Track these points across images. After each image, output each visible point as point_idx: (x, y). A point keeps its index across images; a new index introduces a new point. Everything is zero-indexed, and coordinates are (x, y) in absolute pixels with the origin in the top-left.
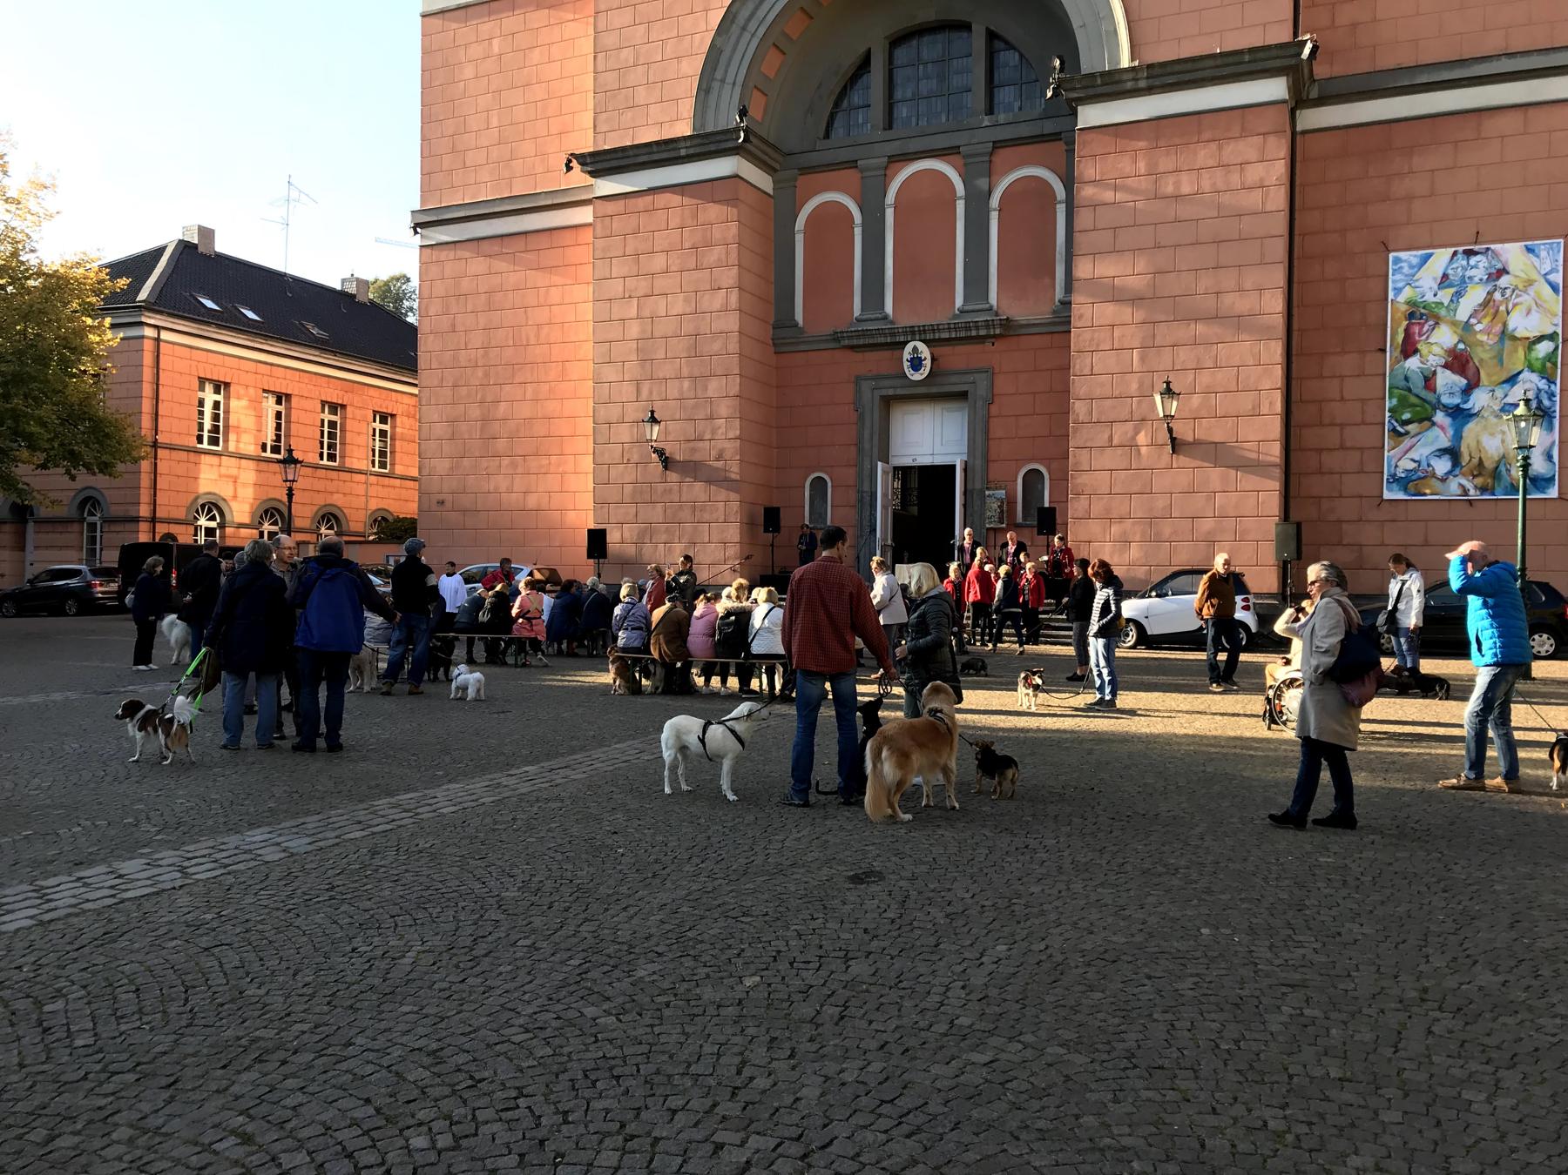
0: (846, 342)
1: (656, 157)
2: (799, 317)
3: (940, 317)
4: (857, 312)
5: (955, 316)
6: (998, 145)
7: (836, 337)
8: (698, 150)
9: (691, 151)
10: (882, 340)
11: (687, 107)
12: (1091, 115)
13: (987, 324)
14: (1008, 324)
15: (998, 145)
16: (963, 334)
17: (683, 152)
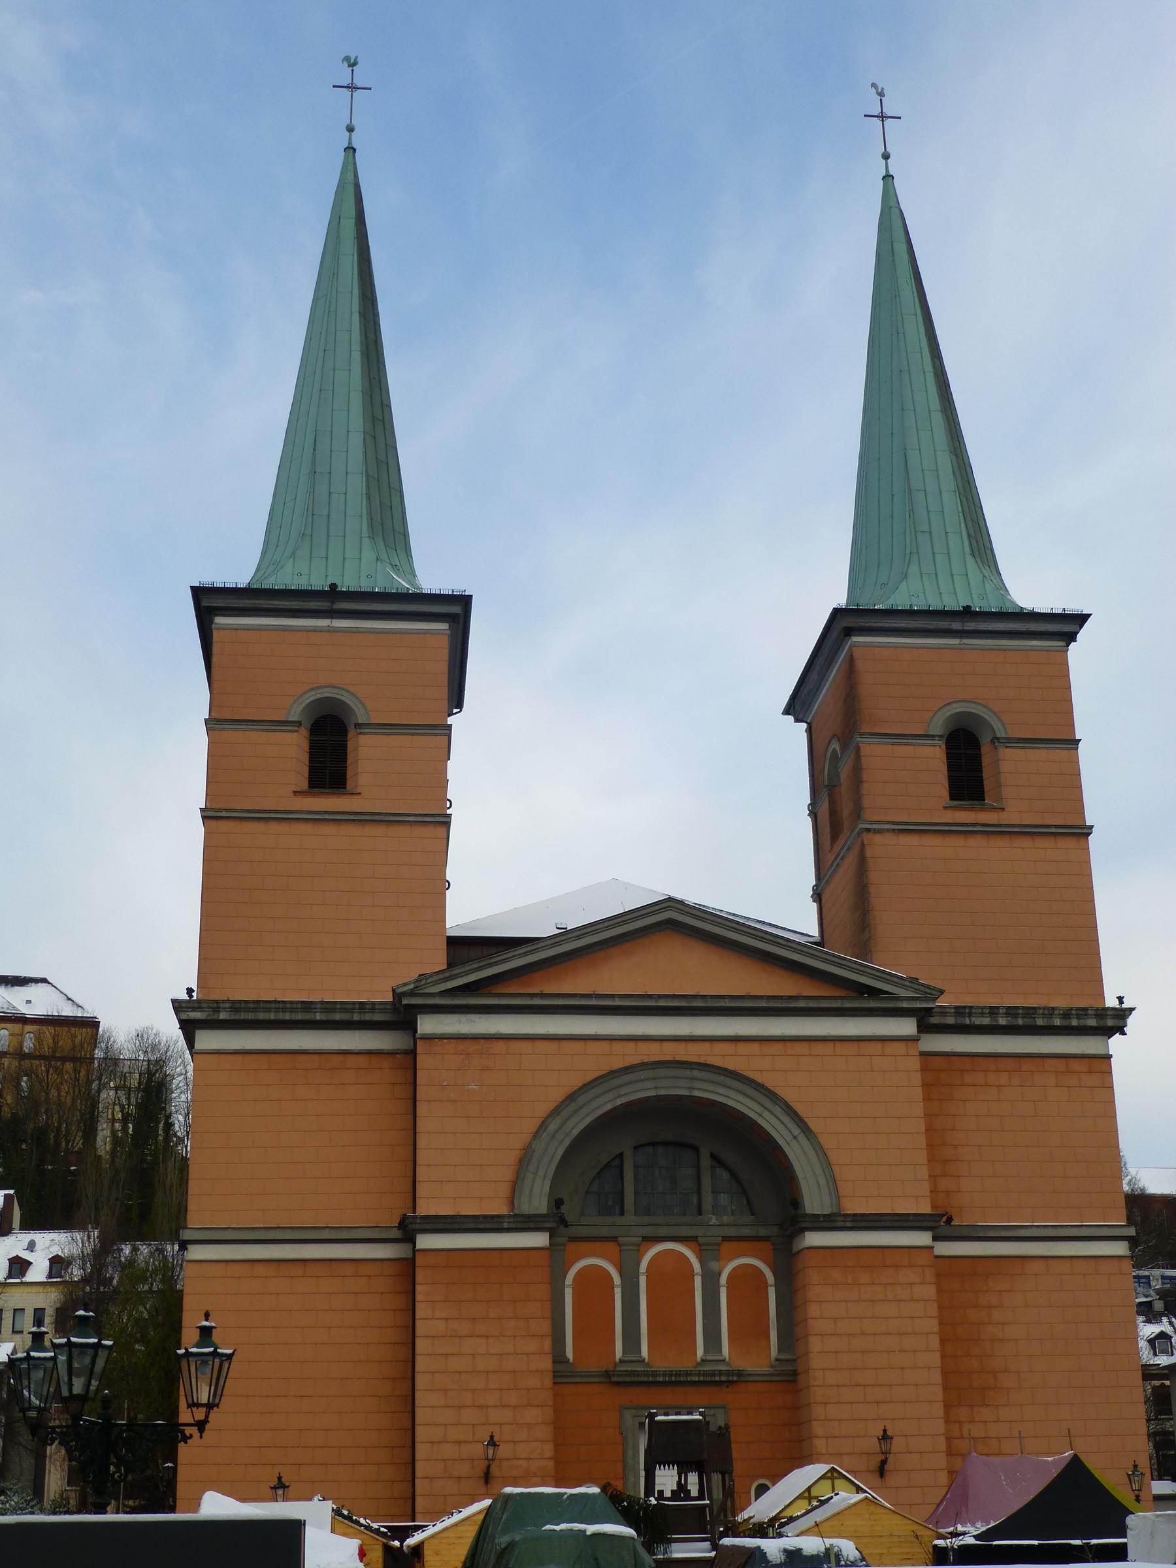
0: (614, 1379)
1: (480, 1226)
2: (570, 1354)
3: (687, 1366)
4: (619, 1353)
5: (698, 1364)
6: (726, 1239)
7: (607, 1374)
8: (519, 1226)
9: (512, 1226)
10: (646, 1379)
11: (504, 1190)
12: (814, 1239)
13: (728, 1373)
14: (740, 1373)
15: (726, 1239)
16: (708, 1379)
17: (505, 1225)
